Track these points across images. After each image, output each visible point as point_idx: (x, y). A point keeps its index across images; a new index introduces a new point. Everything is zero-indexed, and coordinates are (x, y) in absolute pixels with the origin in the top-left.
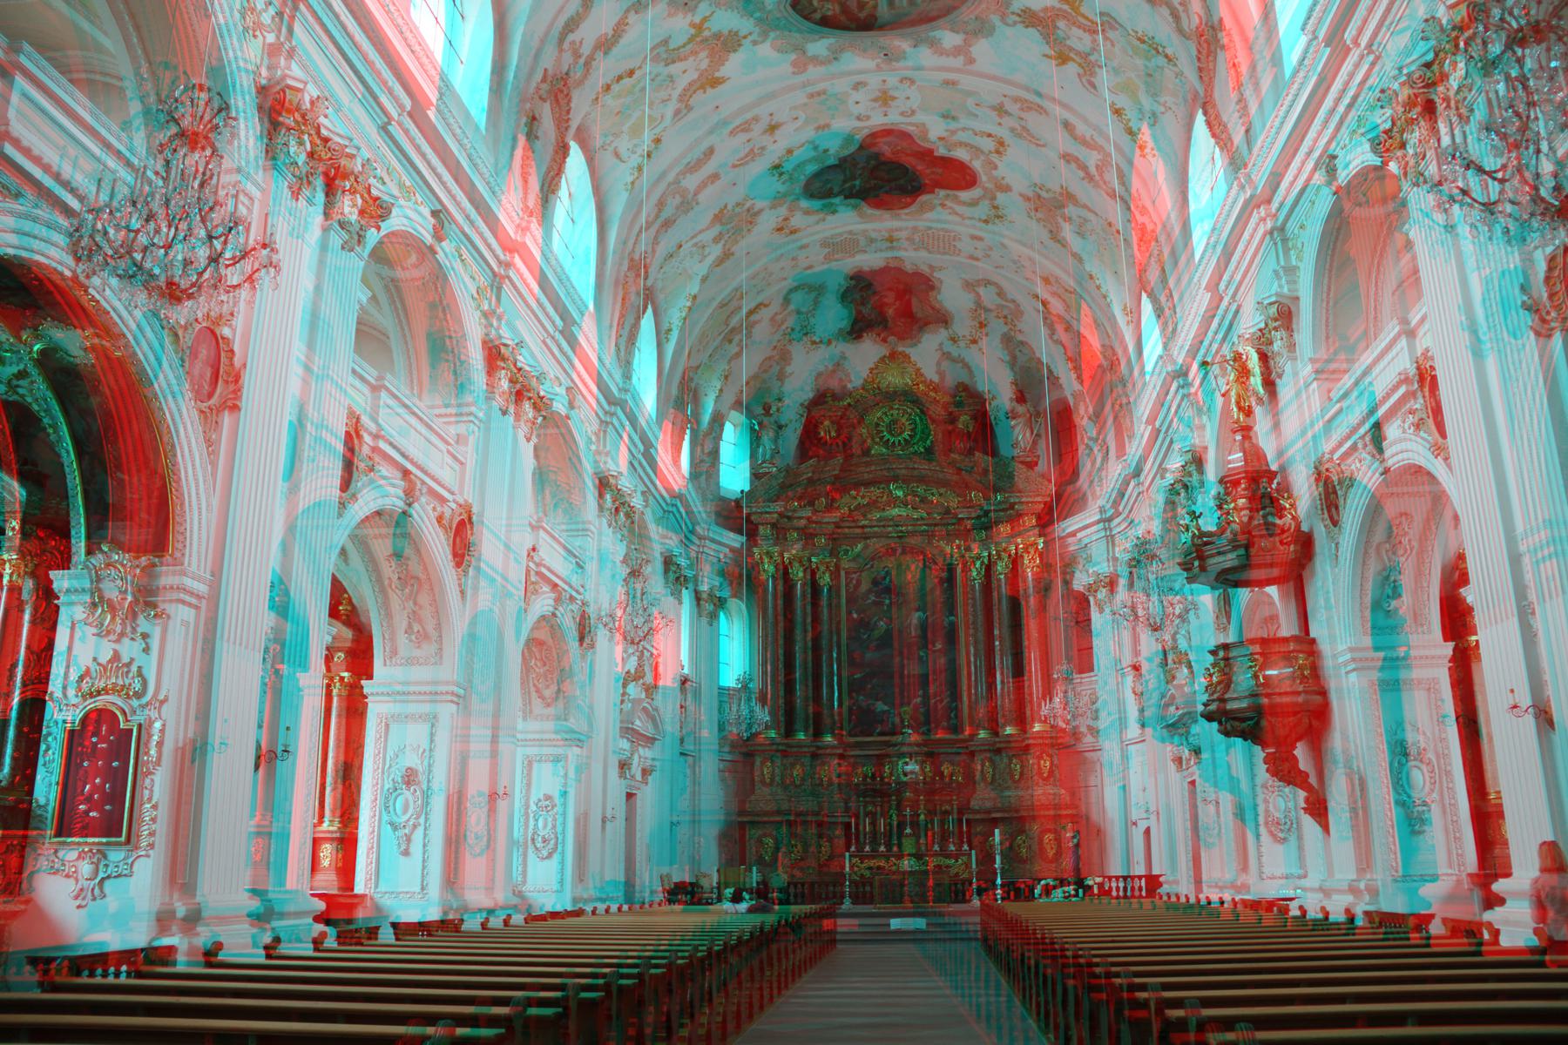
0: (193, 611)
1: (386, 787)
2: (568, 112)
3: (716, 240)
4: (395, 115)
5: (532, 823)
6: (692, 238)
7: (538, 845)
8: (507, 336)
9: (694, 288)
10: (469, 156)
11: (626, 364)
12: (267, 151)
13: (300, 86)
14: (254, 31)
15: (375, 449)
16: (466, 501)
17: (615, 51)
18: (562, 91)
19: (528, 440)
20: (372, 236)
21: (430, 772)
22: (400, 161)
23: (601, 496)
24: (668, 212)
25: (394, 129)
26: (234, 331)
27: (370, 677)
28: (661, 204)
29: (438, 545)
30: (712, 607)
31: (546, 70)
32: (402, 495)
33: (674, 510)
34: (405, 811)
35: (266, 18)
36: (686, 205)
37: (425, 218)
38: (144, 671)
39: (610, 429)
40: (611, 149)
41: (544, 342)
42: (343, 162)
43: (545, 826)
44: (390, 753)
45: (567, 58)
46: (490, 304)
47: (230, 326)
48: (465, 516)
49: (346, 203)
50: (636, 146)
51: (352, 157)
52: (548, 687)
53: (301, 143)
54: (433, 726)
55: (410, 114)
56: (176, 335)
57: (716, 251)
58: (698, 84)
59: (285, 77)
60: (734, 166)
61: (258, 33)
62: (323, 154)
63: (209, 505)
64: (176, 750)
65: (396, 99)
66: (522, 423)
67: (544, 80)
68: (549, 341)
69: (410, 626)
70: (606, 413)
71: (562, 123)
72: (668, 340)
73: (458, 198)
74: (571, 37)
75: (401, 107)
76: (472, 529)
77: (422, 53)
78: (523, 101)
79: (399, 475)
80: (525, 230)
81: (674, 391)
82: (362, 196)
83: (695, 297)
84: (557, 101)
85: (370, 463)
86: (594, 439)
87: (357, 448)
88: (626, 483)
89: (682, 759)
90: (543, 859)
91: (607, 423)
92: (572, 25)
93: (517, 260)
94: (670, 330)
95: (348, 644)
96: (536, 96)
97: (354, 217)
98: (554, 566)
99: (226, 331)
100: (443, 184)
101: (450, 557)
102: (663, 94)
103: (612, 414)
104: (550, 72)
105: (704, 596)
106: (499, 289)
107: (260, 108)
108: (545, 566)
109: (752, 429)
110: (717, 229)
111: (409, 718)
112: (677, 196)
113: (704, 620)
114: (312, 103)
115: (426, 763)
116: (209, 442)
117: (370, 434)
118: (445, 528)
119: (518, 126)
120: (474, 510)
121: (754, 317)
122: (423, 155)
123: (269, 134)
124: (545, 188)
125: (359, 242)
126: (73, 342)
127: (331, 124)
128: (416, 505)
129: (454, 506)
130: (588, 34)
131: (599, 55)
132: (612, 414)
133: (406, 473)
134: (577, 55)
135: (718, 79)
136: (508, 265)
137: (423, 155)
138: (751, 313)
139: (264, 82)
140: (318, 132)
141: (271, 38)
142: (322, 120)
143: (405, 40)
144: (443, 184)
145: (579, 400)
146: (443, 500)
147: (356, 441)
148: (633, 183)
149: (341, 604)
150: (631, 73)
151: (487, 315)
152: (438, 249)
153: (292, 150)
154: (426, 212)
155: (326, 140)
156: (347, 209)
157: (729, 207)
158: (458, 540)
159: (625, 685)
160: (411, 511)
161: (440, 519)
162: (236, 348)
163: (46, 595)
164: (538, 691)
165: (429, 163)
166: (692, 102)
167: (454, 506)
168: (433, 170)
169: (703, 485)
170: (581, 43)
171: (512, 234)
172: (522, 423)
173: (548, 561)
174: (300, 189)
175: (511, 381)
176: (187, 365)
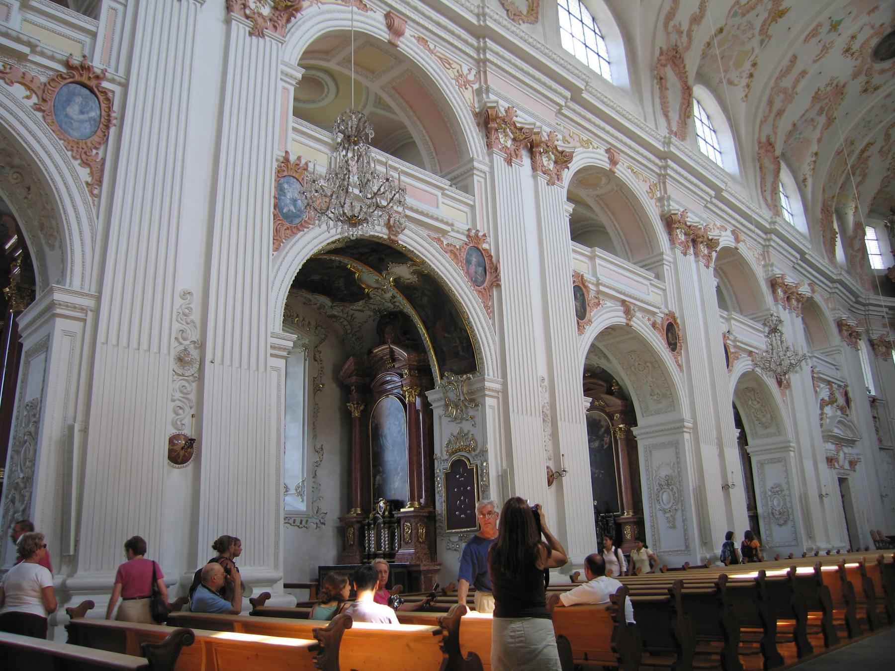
0: (496, 400)
1: (656, 488)
2: (684, 67)
3: (820, 113)
4: (564, 104)
5: (770, 503)
6: (801, 117)
7: (777, 517)
8: (675, 207)
9: (814, 148)
10: (617, 111)
11: (776, 208)
12: (487, 145)
13: (495, 105)
14: (465, 86)
15: (599, 292)
16: (669, 311)
17: (705, 21)
18: (676, 57)
19: (708, 267)
20: (567, 175)
21: (680, 476)
22: (575, 128)
23: (774, 291)
24: (777, 106)
25: (564, 111)
26: (490, 245)
27: (636, 425)
28: (771, 103)
29: (658, 342)
30: (884, 349)
31: (661, 48)
32: (622, 314)
33: (837, 291)
34: (668, 503)
35: (471, 77)
36: (789, 96)
37: (600, 154)
38: (476, 437)
39: (771, 249)
40: (725, 82)
41: (706, 206)
42: (534, 137)
43: (779, 505)
44: (655, 468)
45: (674, 36)
46: (661, 193)
47: (487, 242)
48: (671, 320)
49: (544, 160)
50: (741, 73)
51: (538, 133)
52: (764, 416)
53: (506, 136)
54: (676, 448)
55: (572, 99)
56: (455, 255)
57: (822, 120)
58: (770, 20)
59: (486, 103)
60: (815, 61)
61: (468, 86)
62: (520, 136)
63: (494, 341)
64: (498, 476)
65: (560, 94)
66: (701, 258)
67: (661, 53)
68: (709, 205)
69: (653, 391)
70: (765, 240)
71: (682, 75)
72: (806, 186)
73: (620, 138)
74: (672, 24)
75: (565, 97)
76: (678, 327)
77: (566, 64)
78: (652, 70)
79: (619, 304)
80: (668, 143)
81: (819, 216)
82: (553, 153)
83: (816, 154)
84: (674, 63)
85: (596, 301)
86: (761, 258)
87: (585, 293)
88: (790, 280)
89: (883, 452)
90: (780, 525)
91: (768, 246)
92: (670, 16)
93: (670, 162)
94: (805, 180)
95: (620, 408)
96: (659, 65)
97: (551, 166)
98: (746, 340)
99: (485, 246)
100: (608, 132)
101: (666, 346)
102: (749, 35)
103: (769, 240)
104: (665, 48)
105: (876, 342)
106: (664, 183)
107: (478, 125)
108: (739, 341)
109: (886, 226)
110: (817, 107)
111: (663, 446)
112: (781, 94)
113: (880, 360)
114: (506, 112)
115: (676, 471)
116: (487, 307)
117: (593, 284)
118: (659, 330)
119: (652, 86)
120: (677, 315)
121: (866, 154)
122: (589, 120)
123: (487, 135)
124: (682, 116)
125: (558, 179)
126: (403, 271)
127: (522, 119)
128: (634, 319)
129: (662, 316)
130: (683, 18)
131: (695, 27)
132: (769, 240)
133: (623, 302)
134: (680, 33)
135: (782, 11)
136: (666, 167)
137: (589, 120)
138: (863, 151)
139: (477, 110)
140: (515, 127)
141: (476, 86)
142: (515, 119)
143: (553, 60)
144: (608, 132)
145: (742, 237)
146: (654, 314)
147: (584, 290)
148: (746, 96)
149: (613, 386)
150: (721, 30)
151: (660, 200)
152: (616, 170)
153: (502, 141)
154: (602, 152)
155: (521, 129)
156: (545, 163)
157: (822, 89)
158: (670, 335)
159: (822, 408)
160: (632, 323)
161: (654, 325)
162: (492, 254)
163: (427, 405)
164: (758, 419)
165: (594, 124)
166: (770, 32)
167: (662, 316)
168: (598, 126)
169: (859, 270)
170: (680, 24)
171: (662, 149)
172: (701, 258)
173: (740, 337)
174: (511, 159)
175: (685, 234)
176: (465, 268)
